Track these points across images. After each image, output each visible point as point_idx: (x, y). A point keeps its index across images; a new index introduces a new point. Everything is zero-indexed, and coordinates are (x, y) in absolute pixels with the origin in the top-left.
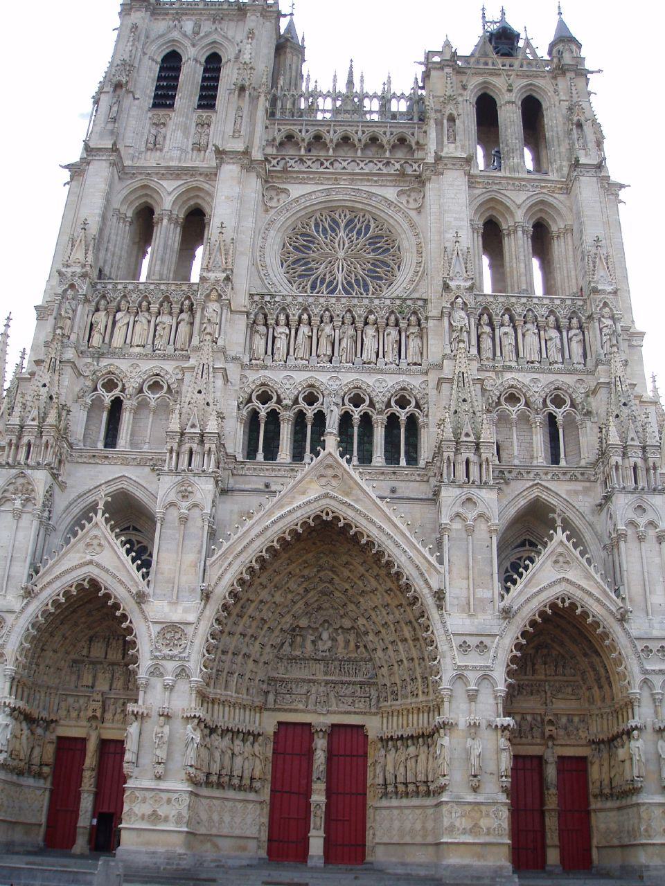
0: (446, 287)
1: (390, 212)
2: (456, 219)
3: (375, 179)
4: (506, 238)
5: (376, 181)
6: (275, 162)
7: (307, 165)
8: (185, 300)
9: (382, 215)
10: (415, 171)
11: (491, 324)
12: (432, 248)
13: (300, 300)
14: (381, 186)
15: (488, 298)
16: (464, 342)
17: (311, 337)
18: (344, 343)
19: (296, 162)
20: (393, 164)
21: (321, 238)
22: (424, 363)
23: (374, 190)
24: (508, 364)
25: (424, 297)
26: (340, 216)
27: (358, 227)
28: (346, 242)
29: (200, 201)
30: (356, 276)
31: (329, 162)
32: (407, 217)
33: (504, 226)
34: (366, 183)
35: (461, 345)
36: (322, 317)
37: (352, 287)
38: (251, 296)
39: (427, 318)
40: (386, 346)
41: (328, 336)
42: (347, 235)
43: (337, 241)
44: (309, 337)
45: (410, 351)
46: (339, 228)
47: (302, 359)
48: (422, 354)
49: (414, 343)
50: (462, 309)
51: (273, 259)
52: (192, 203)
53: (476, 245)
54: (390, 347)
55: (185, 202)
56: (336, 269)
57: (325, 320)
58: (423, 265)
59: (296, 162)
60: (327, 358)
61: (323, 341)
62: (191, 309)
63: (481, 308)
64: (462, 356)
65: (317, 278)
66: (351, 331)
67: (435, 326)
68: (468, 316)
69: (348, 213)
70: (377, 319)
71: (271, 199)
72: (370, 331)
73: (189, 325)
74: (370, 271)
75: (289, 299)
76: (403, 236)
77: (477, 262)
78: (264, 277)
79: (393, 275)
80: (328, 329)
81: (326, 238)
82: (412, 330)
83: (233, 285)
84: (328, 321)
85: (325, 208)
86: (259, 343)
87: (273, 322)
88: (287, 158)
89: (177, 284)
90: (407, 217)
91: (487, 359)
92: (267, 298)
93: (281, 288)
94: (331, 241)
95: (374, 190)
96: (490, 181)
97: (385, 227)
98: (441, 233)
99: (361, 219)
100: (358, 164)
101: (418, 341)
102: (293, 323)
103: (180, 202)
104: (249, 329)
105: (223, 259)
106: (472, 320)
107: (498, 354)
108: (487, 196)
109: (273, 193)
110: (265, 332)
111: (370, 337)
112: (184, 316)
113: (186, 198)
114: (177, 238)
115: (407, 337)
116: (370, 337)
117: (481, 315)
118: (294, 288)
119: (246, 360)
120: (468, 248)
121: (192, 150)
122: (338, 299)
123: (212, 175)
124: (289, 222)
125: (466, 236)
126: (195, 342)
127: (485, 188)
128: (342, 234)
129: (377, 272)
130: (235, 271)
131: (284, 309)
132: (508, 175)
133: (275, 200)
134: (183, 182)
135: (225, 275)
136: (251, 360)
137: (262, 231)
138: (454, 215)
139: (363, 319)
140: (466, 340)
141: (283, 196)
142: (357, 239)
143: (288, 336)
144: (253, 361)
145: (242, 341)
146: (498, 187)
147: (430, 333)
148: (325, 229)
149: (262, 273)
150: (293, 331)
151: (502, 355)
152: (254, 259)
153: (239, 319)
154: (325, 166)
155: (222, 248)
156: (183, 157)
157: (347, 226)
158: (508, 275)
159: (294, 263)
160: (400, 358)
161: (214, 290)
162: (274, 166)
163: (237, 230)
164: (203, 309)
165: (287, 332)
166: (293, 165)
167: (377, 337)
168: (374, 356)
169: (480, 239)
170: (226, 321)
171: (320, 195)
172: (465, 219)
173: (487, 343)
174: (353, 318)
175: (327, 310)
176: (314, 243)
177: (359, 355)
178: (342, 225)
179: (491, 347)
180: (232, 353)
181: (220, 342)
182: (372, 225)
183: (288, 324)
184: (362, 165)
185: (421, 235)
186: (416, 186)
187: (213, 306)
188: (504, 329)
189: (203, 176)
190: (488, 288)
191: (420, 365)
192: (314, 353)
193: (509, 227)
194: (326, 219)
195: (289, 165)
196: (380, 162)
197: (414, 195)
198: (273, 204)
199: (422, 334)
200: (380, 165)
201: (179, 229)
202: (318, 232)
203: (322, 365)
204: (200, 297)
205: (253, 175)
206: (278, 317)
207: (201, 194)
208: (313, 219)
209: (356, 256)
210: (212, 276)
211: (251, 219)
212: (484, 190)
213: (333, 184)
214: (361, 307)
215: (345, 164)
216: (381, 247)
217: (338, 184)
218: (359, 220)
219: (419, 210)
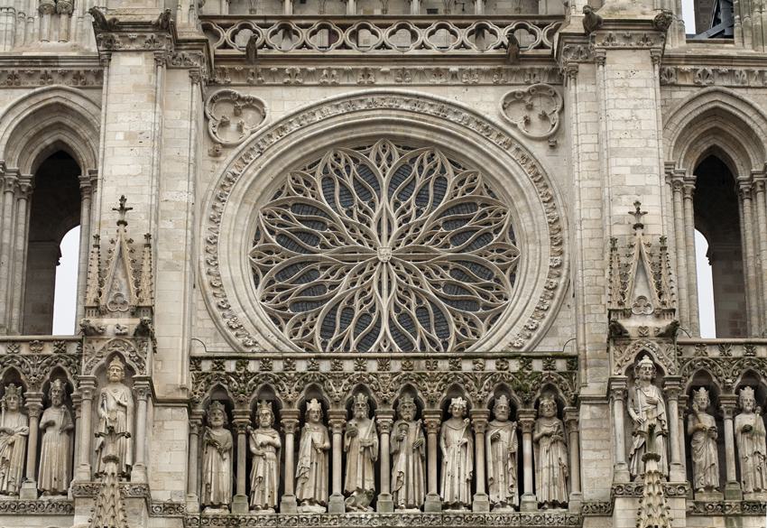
0: (617, 334)
1: (488, 148)
2: (636, 170)
3: (454, 68)
4: (747, 202)
5: (454, 75)
6: (226, 35)
7: (299, 42)
8: (53, 379)
9: (471, 154)
10: (542, 46)
11: (715, 410)
12: (583, 240)
13: (301, 367)
14: (467, 85)
15: (708, 349)
16: (657, 458)
17: (328, 452)
18: (400, 465)
19: (274, 33)
20: (493, 32)
21: (339, 214)
22: (574, 504)
23: (451, 95)
24: (752, 497)
25: (569, 350)
26: (378, 159)
27: (418, 185)
28: (396, 222)
29: (67, 138)
30: (419, 301)
31: (349, 31)
32: (526, 158)
33: (743, 175)
34: (433, 81)
35: (652, 466)
36: (350, 405)
37: (410, 325)
38: (195, 361)
39: (577, 402)
40: (490, 467)
41: (366, 448)
42: (397, 204)
43: (373, 221)
44: (324, 450)
45: (544, 476)
46: (378, 189)
47: (312, 502)
48: (567, 480)
49: (550, 458)
50: (653, 381)
51: (235, 267)
52: (48, 140)
53: (680, 222)
54: (501, 473)
55: (32, 141)
56: (375, 287)
57: (357, 413)
58: (564, 272)
59: (274, 33)
60: (365, 499)
61: (355, 459)
62: (69, 402)
63: (693, 373)
64: (652, 490)
65: (334, 309)
66: (413, 434)
67: (594, 418)
68: (665, 396)
69: (395, 152)
70: (468, 406)
71: (224, 124)
72: (456, 434)
73: (65, 436)
74: (449, 285)
75: (278, 366)
76: (520, 204)
77: (682, 262)
78: (219, 313)
79: (500, 297)
80: (364, 431)
81: (350, 213)
82: (546, 427)
83: (154, 340)
84: (364, 413)
85: (344, 142)
86: (220, 471)
87: (247, 419)
88: (254, 24)
89: (31, 343)
90: (526, 158)
91: (709, 488)
92: (231, 366)
93: (257, 337)
94: (362, 219)
95: (451, 95)
96: (709, 69)
97: (479, 182)
98: (601, 203)
99: (426, 166)
100: (414, 36)
101: (559, 453)
102: (289, 420)
103: (22, 142)
104: (195, 439)
105: (132, 286)
106: (674, 406)
107: (732, 476)
108: (707, 103)
109: (226, 110)
110: (230, 444)
111: (455, 447)
112: (52, 414)
113: (32, 132)
114: (21, 227)
115: (536, 443)
116: (455, 447)
117: (694, 389)
118: (285, 335)
119: (192, 507)
120: (663, 240)
121: (41, 12)
122: (384, 363)
123: (91, 75)
124: (266, 180)
125: (658, 211)
126: (82, 475)
127: (698, 85)
128: (384, 203)
129: (466, 290)
130: (157, 310)
131: (267, 389)
132: (748, 51)
133: (233, 127)
134: (26, 93)
135: (137, 321)
136: (202, 508)
137: (208, 205)
138: (633, 161)
139: (438, 408)
140: (661, 451)
141: (249, 115)
142: (419, 213)
143: (280, 450)
144: (209, 511)
145: (181, 467)
146: (727, 83)
147: (584, 434)
148: (345, 190)
149: (214, 302)
150: (290, 440)
151: (739, 478)
152: (195, 270)
153: (173, 418)
154: (340, 42)
155: (128, 259)
156: (20, 31)
157: (394, 183)
158: (752, 288)
159: (283, 273)
160: (521, 491)
161: (117, 359)
162: (225, 46)
163: (156, 214)
164: (94, 401)
165: (278, 441)
166: (270, 42)
167: (470, 446)
168: (465, 490)
169: (689, 205)
170: (146, 425)
171: (332, 112)
172: (656, 170)
173: (707, 453)
174: (418, 403)
175: (361, 389)
176: (323, 225)
177: (433, 490)
178: (385, 181)
179: (715, 460)
180: (161, 495)
181: (137, 476)
182: (452, 180)
183: (277, 425)
184: (423, 35)
185: (559, 202)
186: (544, 82)
187: (120, 393)
188: (745, 420)
189: (69, 79)
190: (708, 331)
191: (565, 506)
192: (337, 489)
193: (752, 175)
194: (348, 168)
195: (259, 41)
196: (462, 26)
197: (540, 105)
198: (229, 136)
199: (567, 435)
200: (463, 35)
201: (23, 204)
202: (331, 199)
203: (355, 514)
204: (88, 368)
205: (183, 76)
206: (255, 408)
207: (68, 121)
208: (319, 169)
209: (419, 254)
210: (109, 324)
211: (184, 185)
212: (697, 91)
213: (360, 85)
214: (432, 379)
215: (384, 34)
216: (472, 231)
217: (372, 85)
218: (421, 168)
219: (553, 142)
